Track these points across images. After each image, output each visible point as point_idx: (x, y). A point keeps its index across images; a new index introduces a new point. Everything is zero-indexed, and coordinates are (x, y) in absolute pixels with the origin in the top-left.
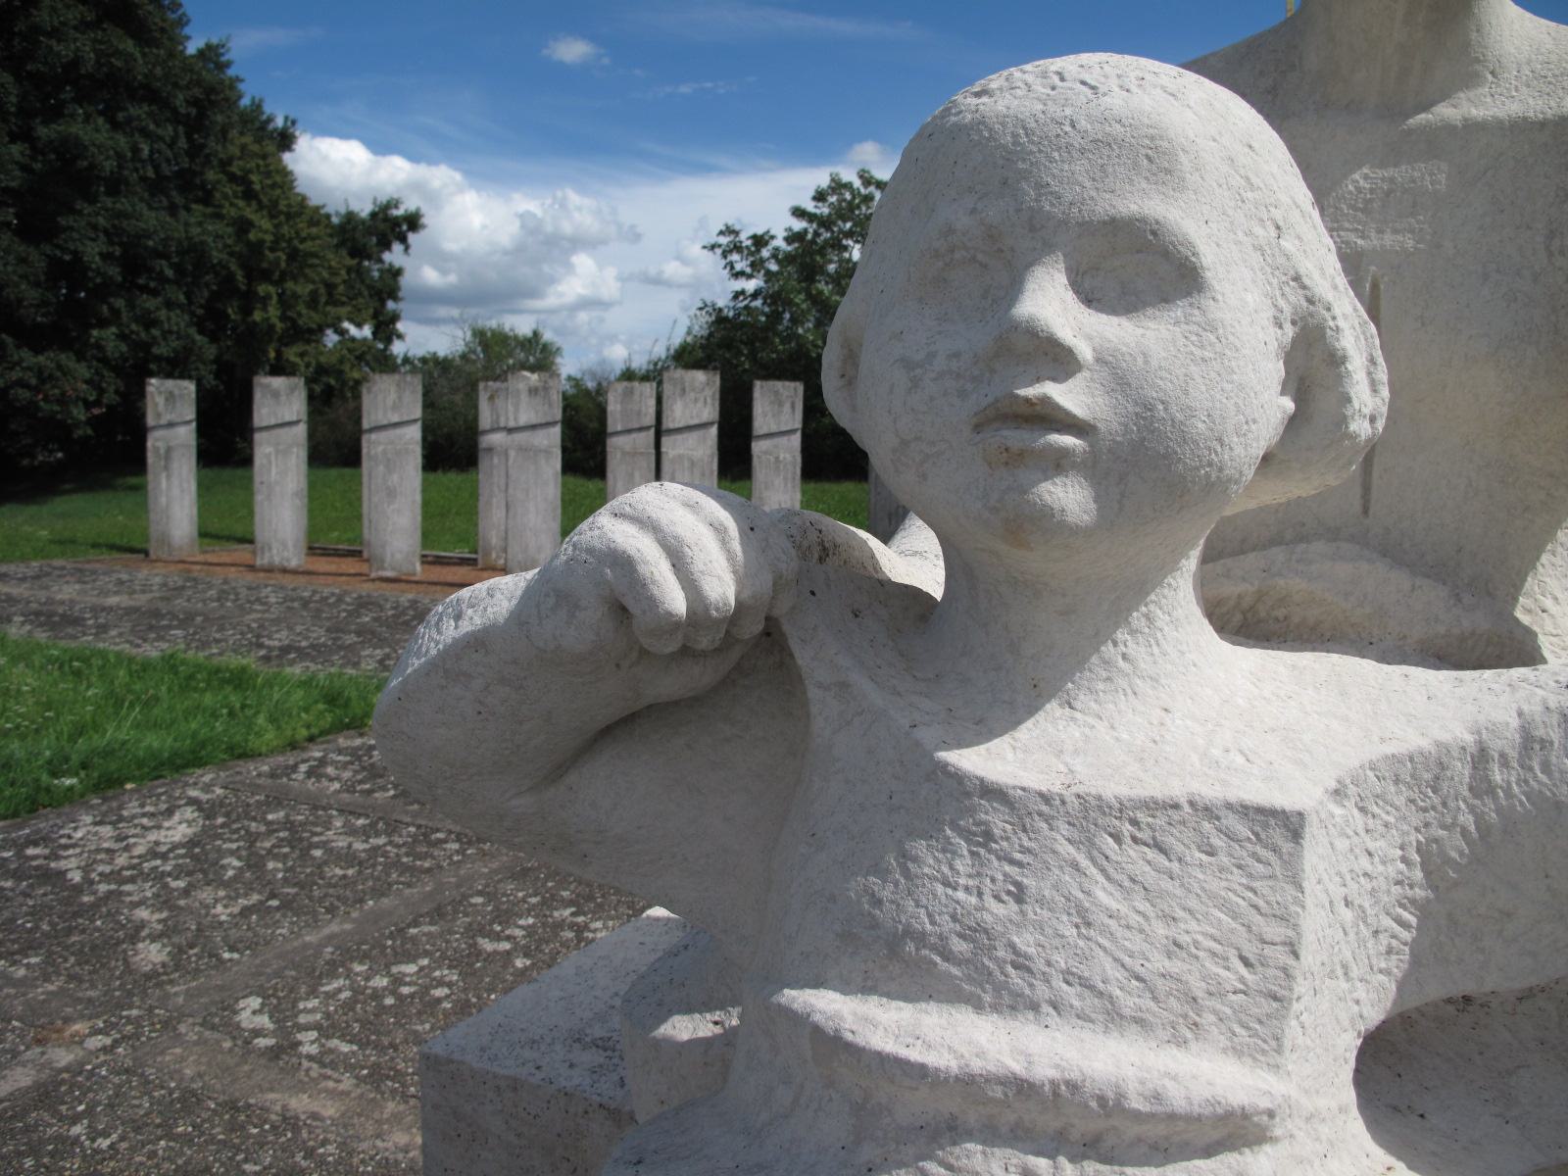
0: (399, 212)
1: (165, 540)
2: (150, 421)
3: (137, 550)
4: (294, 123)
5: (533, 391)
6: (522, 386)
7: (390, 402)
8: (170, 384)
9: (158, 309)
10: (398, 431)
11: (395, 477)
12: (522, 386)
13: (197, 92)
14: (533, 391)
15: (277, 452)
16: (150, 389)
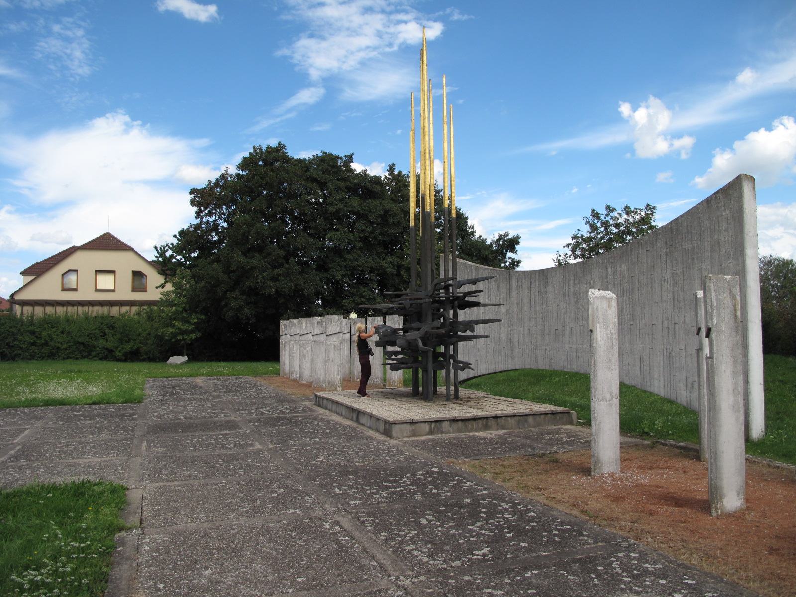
0: (511, 237)
1: (284, 370)
2: (281, 334)
3: (277, 373)
4: (460, 210)
5: (318, 323)
6: (315, 322)
7: (304, 328)
8: (285, 322)
9: (364, 291)
10: (307, 336)
11: (306, 351)
12: (315, 322)
13: (382, 212)
14: (318, 323)
15: (295, 343)
16: (281, 324)
